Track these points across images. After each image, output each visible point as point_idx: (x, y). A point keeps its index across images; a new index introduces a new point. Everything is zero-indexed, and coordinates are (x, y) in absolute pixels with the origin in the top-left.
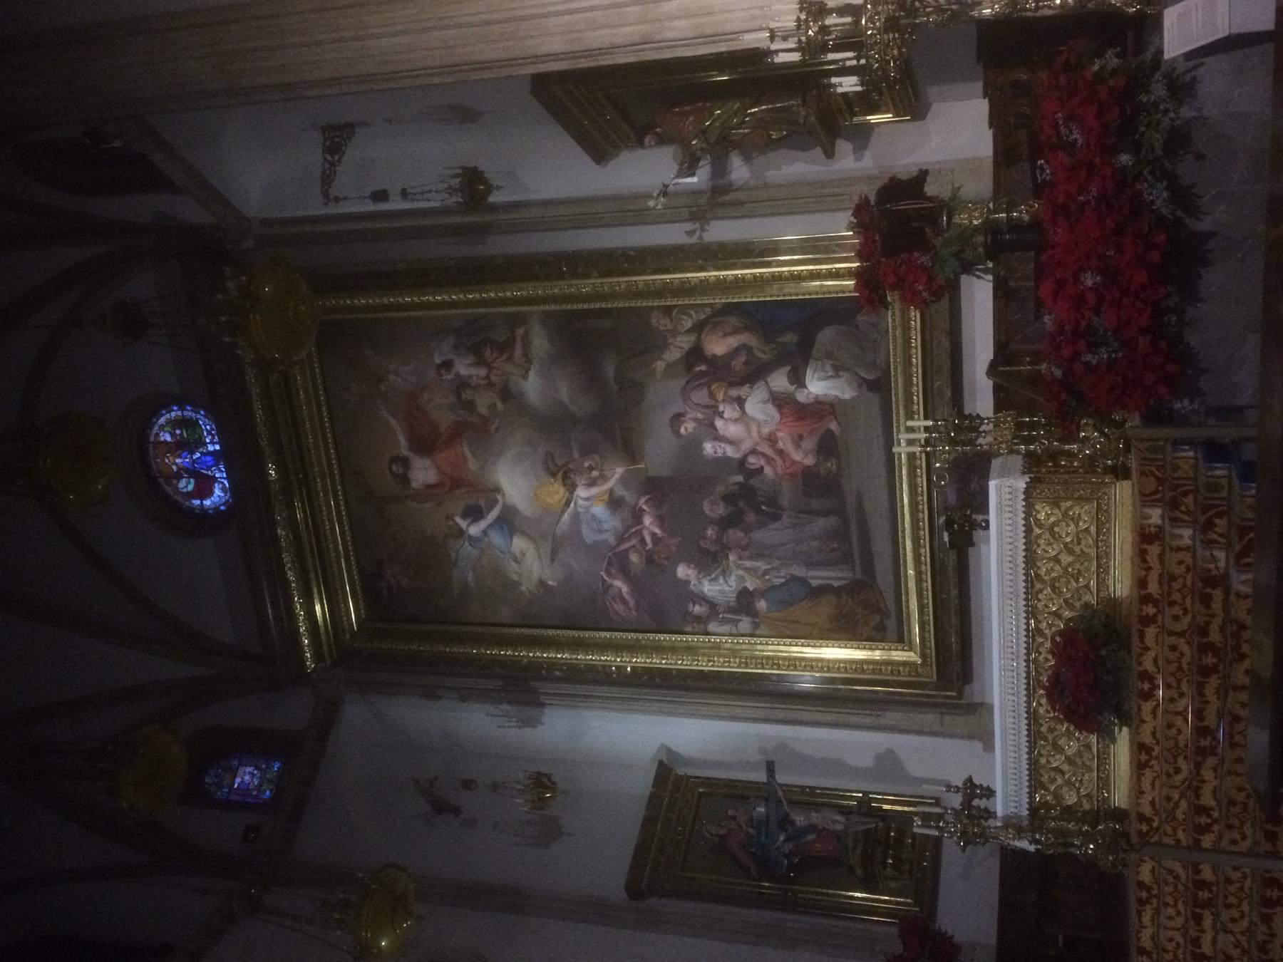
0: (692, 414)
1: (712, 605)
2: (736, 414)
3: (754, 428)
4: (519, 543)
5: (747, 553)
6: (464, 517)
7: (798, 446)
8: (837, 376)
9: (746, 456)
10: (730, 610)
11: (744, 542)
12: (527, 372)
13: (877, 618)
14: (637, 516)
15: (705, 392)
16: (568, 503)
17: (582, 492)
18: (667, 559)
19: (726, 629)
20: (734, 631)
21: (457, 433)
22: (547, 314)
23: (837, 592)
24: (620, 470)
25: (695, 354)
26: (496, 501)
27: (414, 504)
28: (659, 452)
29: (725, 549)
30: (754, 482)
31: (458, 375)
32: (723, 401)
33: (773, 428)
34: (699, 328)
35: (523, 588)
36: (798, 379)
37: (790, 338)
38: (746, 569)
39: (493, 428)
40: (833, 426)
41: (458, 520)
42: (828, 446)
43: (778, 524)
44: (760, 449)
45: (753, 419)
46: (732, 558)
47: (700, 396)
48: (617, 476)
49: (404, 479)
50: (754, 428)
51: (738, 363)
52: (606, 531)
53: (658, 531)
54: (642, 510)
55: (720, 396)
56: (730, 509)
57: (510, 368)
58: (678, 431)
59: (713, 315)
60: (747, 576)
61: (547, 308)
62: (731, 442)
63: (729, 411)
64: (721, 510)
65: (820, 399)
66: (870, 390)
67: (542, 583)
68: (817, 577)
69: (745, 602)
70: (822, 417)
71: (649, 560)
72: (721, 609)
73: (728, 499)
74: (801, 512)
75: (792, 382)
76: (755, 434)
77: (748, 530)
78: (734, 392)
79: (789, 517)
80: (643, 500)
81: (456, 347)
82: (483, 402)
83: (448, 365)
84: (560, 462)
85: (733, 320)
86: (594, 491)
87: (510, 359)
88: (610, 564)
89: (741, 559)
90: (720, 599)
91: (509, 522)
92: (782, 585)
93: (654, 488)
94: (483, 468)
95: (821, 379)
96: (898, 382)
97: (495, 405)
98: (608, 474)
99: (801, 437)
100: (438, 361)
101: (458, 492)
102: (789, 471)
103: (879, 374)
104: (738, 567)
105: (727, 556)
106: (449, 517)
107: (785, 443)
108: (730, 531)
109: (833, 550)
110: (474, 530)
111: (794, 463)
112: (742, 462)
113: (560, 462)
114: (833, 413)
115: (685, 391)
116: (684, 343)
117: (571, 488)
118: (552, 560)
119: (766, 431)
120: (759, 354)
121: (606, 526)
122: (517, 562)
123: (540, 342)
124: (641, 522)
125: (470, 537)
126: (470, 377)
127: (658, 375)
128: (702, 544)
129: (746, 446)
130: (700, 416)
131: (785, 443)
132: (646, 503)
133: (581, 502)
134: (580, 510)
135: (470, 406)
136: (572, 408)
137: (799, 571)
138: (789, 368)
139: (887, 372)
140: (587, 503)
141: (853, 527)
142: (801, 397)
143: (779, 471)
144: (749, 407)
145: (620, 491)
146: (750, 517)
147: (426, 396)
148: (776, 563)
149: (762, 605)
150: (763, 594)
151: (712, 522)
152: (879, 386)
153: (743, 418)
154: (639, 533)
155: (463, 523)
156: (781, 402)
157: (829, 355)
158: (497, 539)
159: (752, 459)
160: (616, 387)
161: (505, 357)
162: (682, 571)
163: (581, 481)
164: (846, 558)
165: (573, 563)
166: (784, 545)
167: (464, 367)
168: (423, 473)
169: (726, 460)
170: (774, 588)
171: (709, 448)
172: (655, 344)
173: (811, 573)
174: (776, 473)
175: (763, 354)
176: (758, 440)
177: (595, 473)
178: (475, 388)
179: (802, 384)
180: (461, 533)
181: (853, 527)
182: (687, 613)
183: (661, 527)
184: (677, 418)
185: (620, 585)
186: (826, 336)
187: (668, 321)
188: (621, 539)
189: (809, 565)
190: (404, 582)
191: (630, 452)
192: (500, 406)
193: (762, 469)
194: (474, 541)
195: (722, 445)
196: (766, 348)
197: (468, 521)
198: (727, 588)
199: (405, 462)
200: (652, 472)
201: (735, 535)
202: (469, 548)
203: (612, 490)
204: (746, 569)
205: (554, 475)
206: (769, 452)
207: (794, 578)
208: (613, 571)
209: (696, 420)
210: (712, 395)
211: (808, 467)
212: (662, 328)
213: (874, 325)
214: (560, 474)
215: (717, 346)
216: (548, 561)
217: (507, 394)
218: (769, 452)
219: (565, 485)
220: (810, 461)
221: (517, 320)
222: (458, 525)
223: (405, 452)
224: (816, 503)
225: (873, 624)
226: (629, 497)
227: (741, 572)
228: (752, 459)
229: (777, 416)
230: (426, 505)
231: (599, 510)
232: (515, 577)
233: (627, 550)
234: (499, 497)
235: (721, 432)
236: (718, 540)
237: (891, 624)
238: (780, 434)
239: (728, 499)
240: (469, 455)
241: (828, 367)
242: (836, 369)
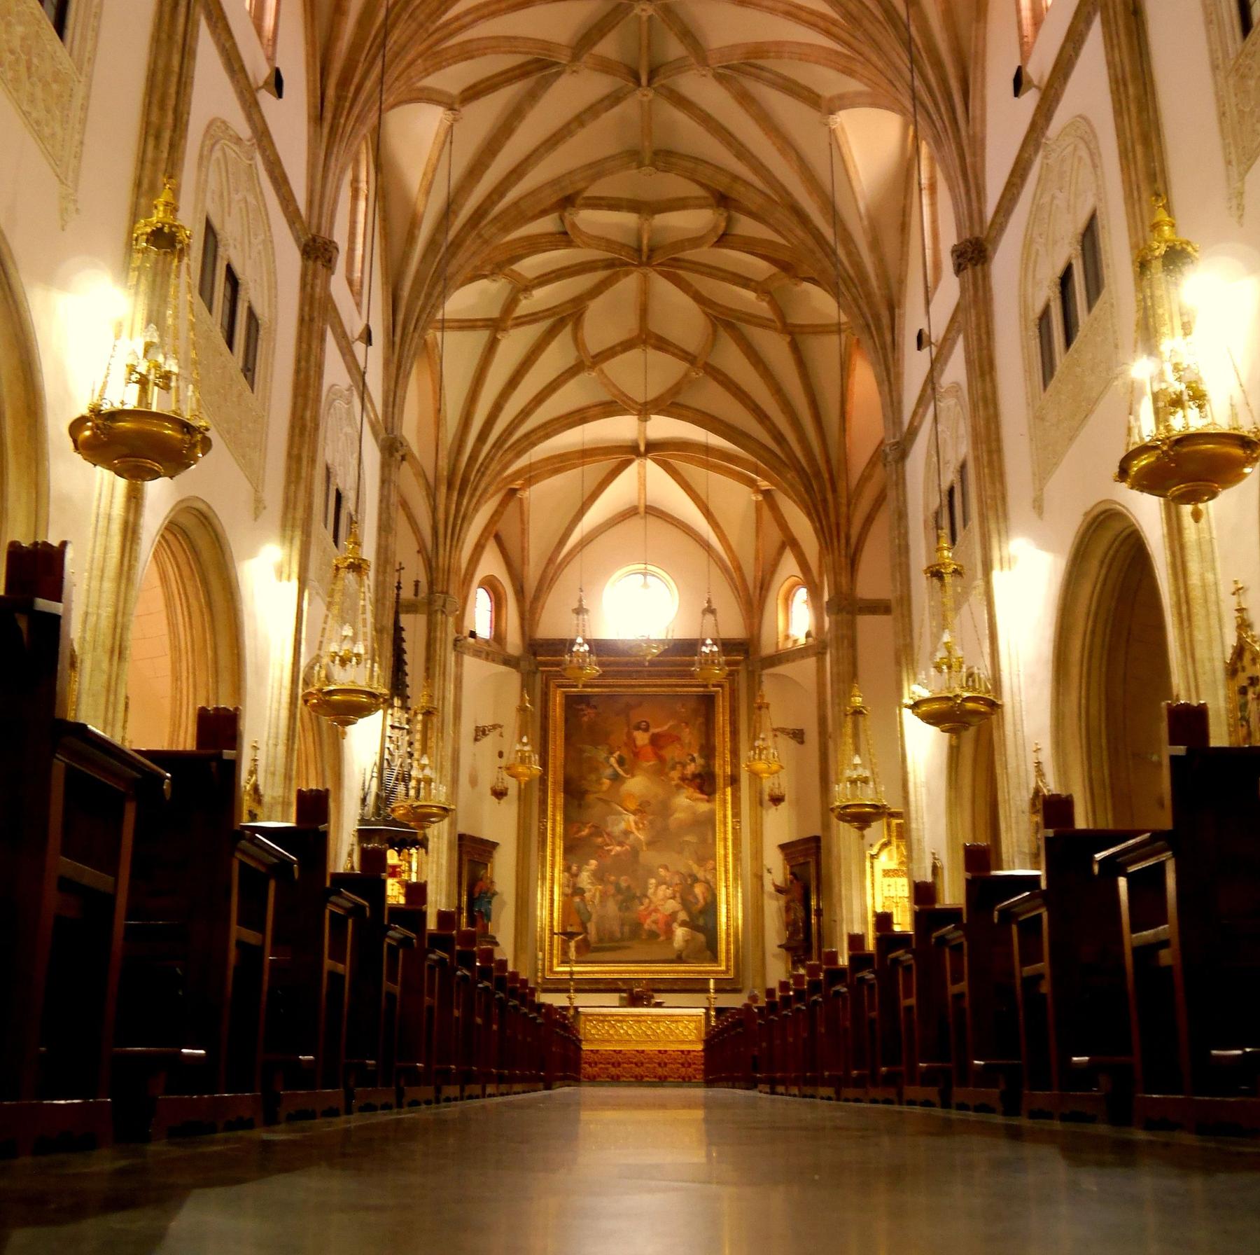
1: (576, 875)
6: (620, 756)
14: (621, 844)
17: (632, 818)
21: (661, 759)
34: (707, 882)
36: (683, 924)
40: (662, 938)
42: (653, 935)
47: (676, 880)
49: (638, 728)
63: (669, 892)
64: (623, 885)
69: (579, 891)
71: (600, 847)
73: (628, 888)
83: (693, 760)
86: (633, 824)
90: (579, 879)
91: (616, 778)
100: (696, 755)
106: (619, 748)
107: (654, 916)
110: (613, 760)
112: (646, 896)
115: (678, 873)
116: (701, 874)
117: (634, 813)
129: (654, 899)
131: (654, 916)
135: (673, 768)
137: (594, 917)
142: (675, 925)
145: (632, 837)
146: (620, 897)
149: (577, 899)
152: (679, 959)
153: (666, 898)
155: (616, 754)
156: (673, 917)
158: (609, 771)
162: (593, 863)
163: (636, 818)
164: (601, 940)
168: (642, 738)
169: (646, 888)
170: (586, 905)
180: (612, 753)
184: (666, 868)
185: (585, 832)
186: (701, 937)
188: (608, 834)
190: (585, 719)
192: (673, 783)
194: (607, 759)
199: (646, 730)
200: (642, 855)
201: (611, 889)
207: (590, 915)
215: (699, 890)
220: (646, 927)
224: (627, 929)
231: (623, 826)
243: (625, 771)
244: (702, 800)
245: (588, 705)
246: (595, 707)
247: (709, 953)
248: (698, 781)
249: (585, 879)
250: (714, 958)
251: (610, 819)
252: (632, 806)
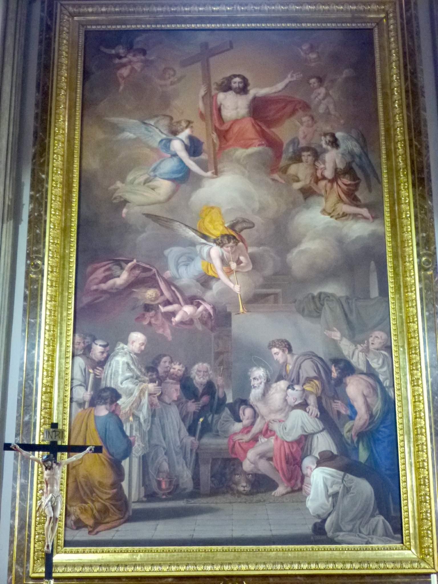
0: (291, 360)
1: (102, 364)
2: (291, 400)
3: (279, 416)
4: (164, 187)
5: (156, 400)
6: (191, 138)
7: (262, 456)
8: (328, 496)
9: (251, 407)
10: (97, 381)
11: (167, 399)
12: (329, 214)
13: (90, 522)
15: (313, 374)
16: (204, 237)
17: (215, 251)
18: (150, 324)
19: (78, 375)
20: (76, 382)
21: (273, 144)
22: (381, 239)
23: (117, 484)
24: (237, 288)
25: (348, 369)
26: (206, 170)
27: (202, 92)
28: (253, 326)
29: (160, 380)
30: (226, 412)
31: (325, 151)
32: (304, 390)
33: (278, 433)
34: (371, 373)
35: (119, 184)
36: (325, 460)
37: (363, 455)
38: (140, 398)
39: (276, 176)
40: (281, 490)
41: (187, 132)
42: (261, 484)
43: (184, 431)
44: (258, 420)
45: (287, 416)
46: (151, 387)
47: (308, 369)
48: (231, 285)
49: (226, 87)
50: (279, 416)
51: (339, 406)
52: (177, 270)
53: (177, 318)
54: (198, 305)
55: (308, 388)
56: (201, 390)
57: (333, 198)
58: (275, 346)
59: (383, 389)
60: (132, 399)
61: (388, 239)
62: (265, 394)
63: (294, 395)
65: (306, 480)
66: (315, 525)
67: (125, 202)
68: (131, 466)
70: (289, 480)
71: (147, 308)
72: (98, 372)
73: (210, 388)
74: (197, 454)
75: (321, 454)
76: (273, 417)
77: (178, 403)
78: (312, 400)
79: (192, 443)
80: (209, 307)
81: (351, 154)
82: (301, 171)
83: (335, 143)
84: (243, 234)
85: (377, 406)
86: (217, 263)
87: (340, 200)
88: (145, 270)
89: (150, 395)
90: (109, 370)
91: (183, 178)
92: (123, 433)
93: (221, 319)
94: (238, 161)
95: (325, 480)
96: (324, 551)
97: (298, 181)
98: (233, 277)
99: (270, 459)
100: (339, 135)
101: (214, 136)
102: (237, 445)
103: (330, 534)
104: (142, 391)
105: (152, 381)
106: (189, 123)
107: (265, 444)
108: (178, 386)
109: (159, 483)
110: (177, 146)
111: (245, 451)
112: (245, 402)
113: (243, 234)
114: (293, 491)
115: (312, 356)
116: (358, 360)
117: (220, 242)
118: (148, 215)
119: (276, 427)
120: (348, 426)
121: (182, 269)
122: (146, 182)
123: (358, 229)
124: (187, 303)
125: (170, 141)
126: (324, 162)
127: (327, 333)
128: (165, 359)
129: (261, 408)
130: (289, 367)
131: (265, 444)
132: (206, 310)
133: (206, 249)
134: (198, 248)
135: (297, 159)
136: (295, 251)
138: (335, 452)
139: (332, 542)
140: (205, 255)
141: (181, 503)
142: (308, 463)
143: (237, 438)
144: (299, 412)
145: (216, 287)
146: (192, 407)
147: (305, 119)
148: (146, 427)
149: (102, 411)
150: (114, 413)
151: (187, 370)
152: (319, 535)
153: (288, 407)
154: (176, 301)
155: (184, 135)
156: (304, 442)
157: (347, 490)
158: (169, 165)
159: (248, 412)
160: (316, 294)
161: (343, 196)
162: (137, 339)
163: (226, 251)
164: (151, 496)
165: (144, 235)
166: (164, 438)
167: (332, 159)
168: (234, 106)
170: (120, 425)
171: (259, 373)
172: (356, 330)
173: (136, 462)
174: (235, 434)
175: (349, 429)
176: (267, 419)
177: (233, 266)
178: (314, 165)
179: (319, 463)
180: (175, 133)
181: (181, 503)
182: (94, 339)
183: (182, 322)
185: (123, 278)
186: (364, 488)
187: (377, 346)
188: (169, 283)
189: (144, 460)
190: (125, 72)
191: (255, 300)
192: (297, 186)
193: (239, 420)
194: (166, 144)
195: (262, 386)
196: (353, 432)
197: (187, 142)
198: (120, 379)
199: (243, 90)
200: (236, 320)
201: (174, 391)
202: (159, 139)
203: (218, 279)
204: (140, 398)
205: (232, 227)
206: (255, 429)
207: (130, 445)
208: (137, 272)
209: (285, 363)
210: (309, 380)
211: (241, 464)
212: (371, 340)
213: (374, 531)
214: (233, 233)
215: (355, 389)
216: (146, 212)
217: (307, 193)
218: (255, 429)
219: (223, 236)
220: (247, 466)
221: (376, 210)
222: (183, 130)
223: (253, 92)
224: (205, 471)
225: (83, 517)
226: (209, 295)
227: (136, 393)
228: (248, 412)
229: (290, 439)
230: (201, 105)
231: (198, 267)
232: (130, 177)
233: (158, 287)
234: (209, 174)
235: (274, 385)
236: (168, 374)
237: (82, 535)
238: (272, 440)
239: (210, 388)
240: (251, 150)
241: (336, 488)
242: (335, 495)
243: (199, 164)
244: (355, 216)
245: (130, 48)
246: (144, 52)
247: (380, 519)
248: (346, 180)
249: (120, 371)
250: (396, 530)
251: (173, 253)
252: (217, 230)
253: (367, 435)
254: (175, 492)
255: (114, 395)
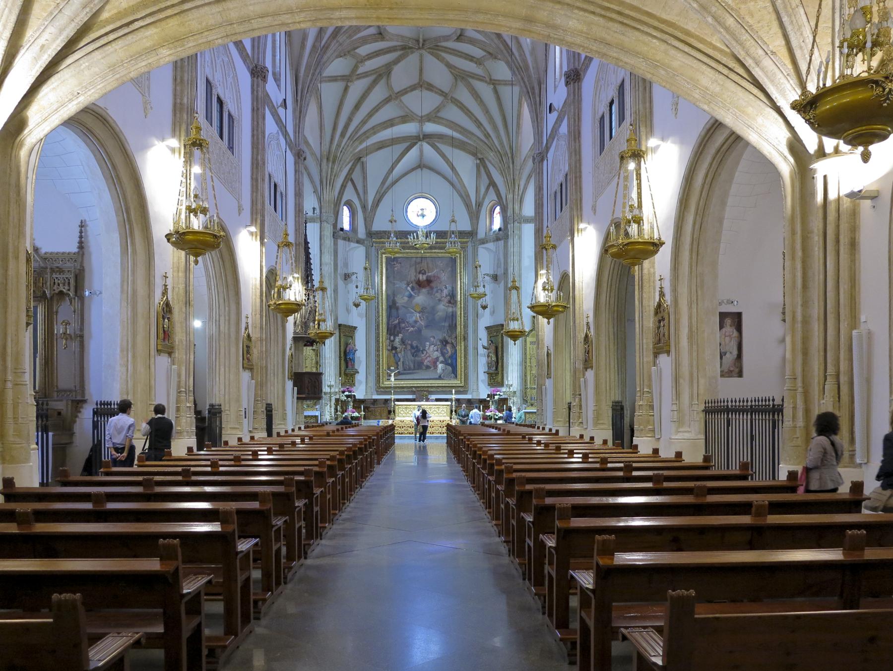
1: (393, 341)
4: (406, 299)
14: (413, 327)
25: (447, 342)
34: (452, 343)
42: (428, 367)
116: (449, 341)
131: (429, 359)
152: (440, 378)
156: (437, 359)
158: (407, 293)
175: (447, 356)
186: (450, 368)
191: (427, 327)
201: (409, 347)
231: (414, 318)
253: (450, 357)
254: (410, 369)
255: (396, 348)
